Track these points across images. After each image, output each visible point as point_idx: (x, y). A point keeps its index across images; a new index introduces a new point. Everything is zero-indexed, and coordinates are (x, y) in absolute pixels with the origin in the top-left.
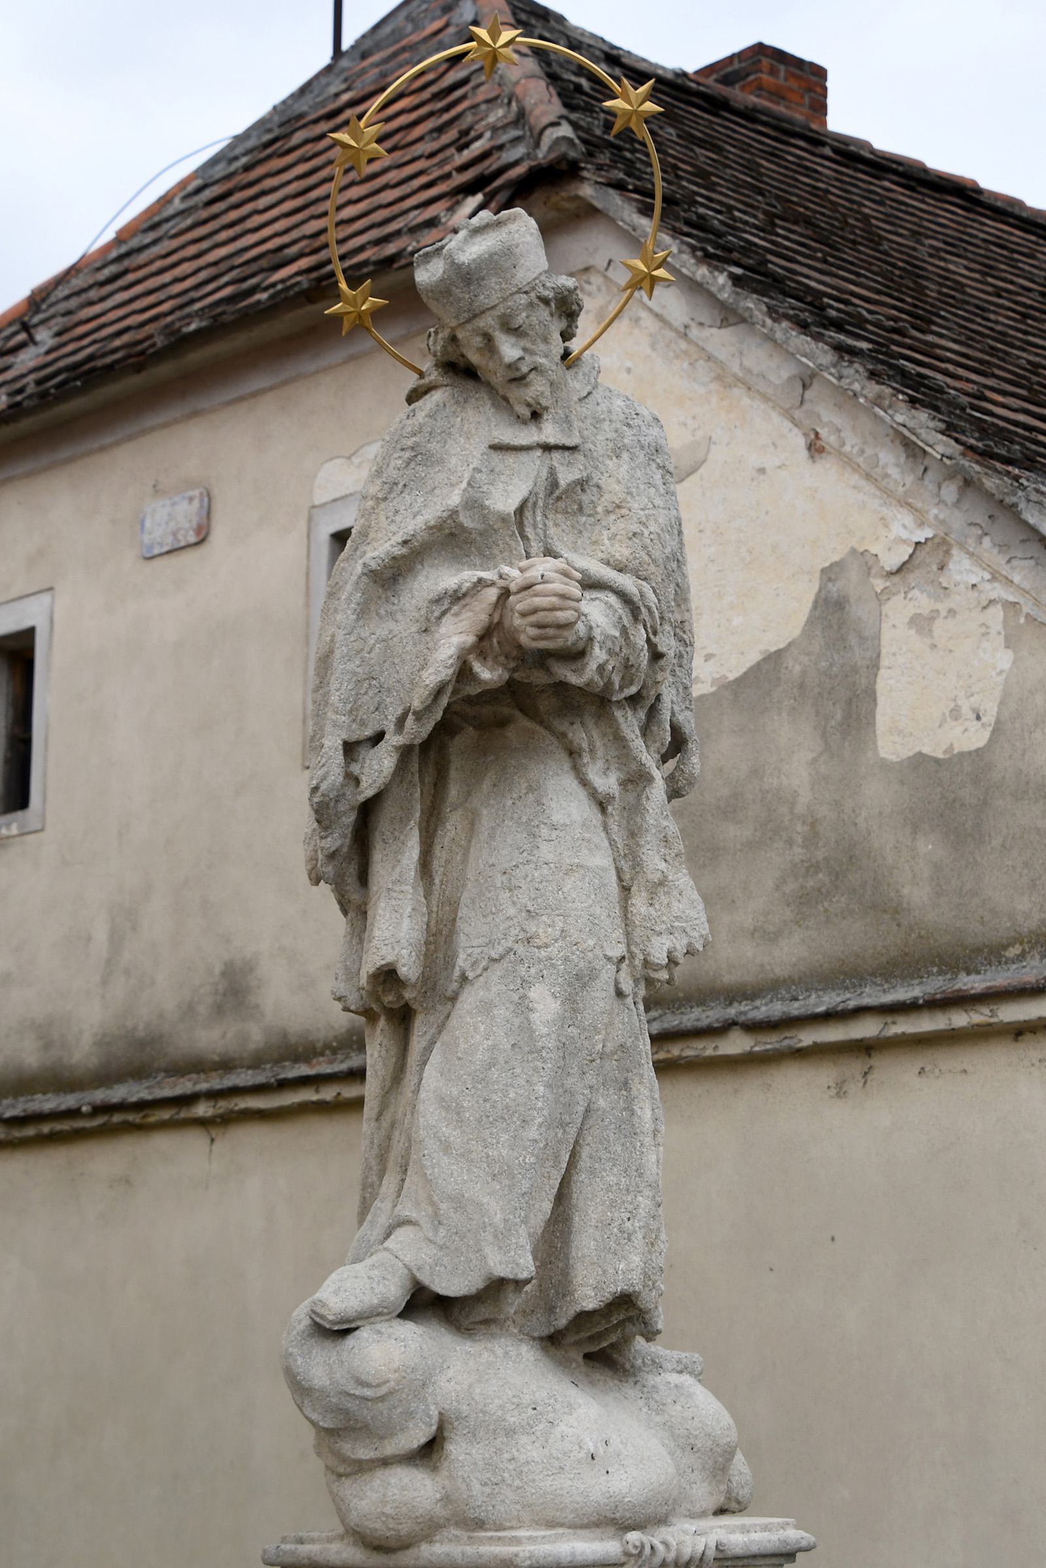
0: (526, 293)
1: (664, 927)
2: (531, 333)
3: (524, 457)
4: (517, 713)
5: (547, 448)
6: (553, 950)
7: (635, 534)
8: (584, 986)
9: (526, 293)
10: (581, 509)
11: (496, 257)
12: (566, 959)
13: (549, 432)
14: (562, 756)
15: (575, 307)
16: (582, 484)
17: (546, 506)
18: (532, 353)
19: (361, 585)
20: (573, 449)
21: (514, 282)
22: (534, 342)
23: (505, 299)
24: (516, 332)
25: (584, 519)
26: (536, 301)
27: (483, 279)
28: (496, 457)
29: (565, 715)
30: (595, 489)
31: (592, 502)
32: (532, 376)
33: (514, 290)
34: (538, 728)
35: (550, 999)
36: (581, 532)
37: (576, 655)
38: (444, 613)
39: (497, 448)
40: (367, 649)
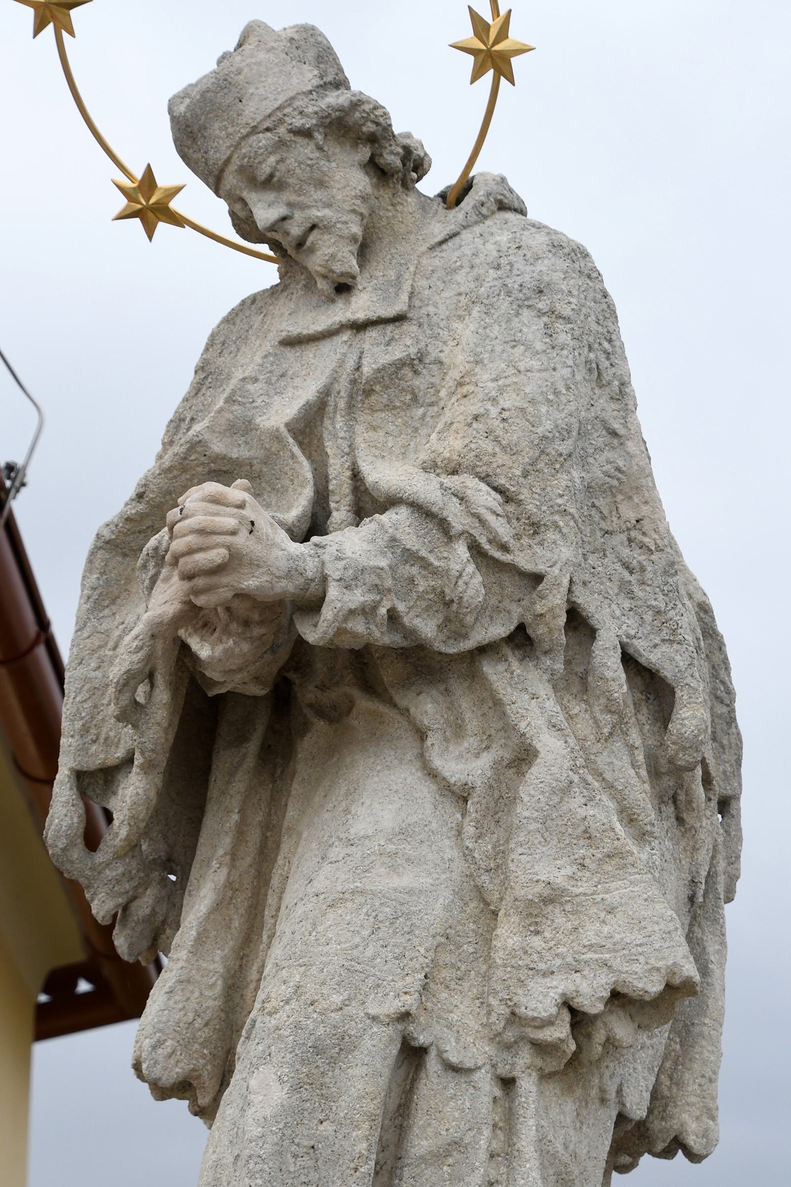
0: (268, 129)
1: (558, 962)
2: (291, 181)
3: (326, 347)
4: (356, 693)
5: (359, 327)
6: (282, 1016)
7: (476, 418)
8: (333, 1062)
9: (268, 129)
10: (415, 398)
11: (209, 95)
12: (297, 1026)
13: (361, 305)
14: (408, 740)
15: (370, 127)
16: (414, 363)
17: (350, 407)
18: (303, 207)
19: (97, 564)
20: (399, 319)
21: (243, 120)
22: (299, 192)
23: (237, 146)
24: (270, 183)
25: (421, 411)
26: (288, 137)
27: (205, 128)
28: (291, 354)
29: (413, 684)
30: (434, 367)
31: (433, 385)
32: (311, 238)
33: (244, 132)
34: (382, 708)
35: (275, 1086)
36: (416, 430)
37: (312, 605)
38: (154, 580)
39: (293, 342)
40: (111, 644)
